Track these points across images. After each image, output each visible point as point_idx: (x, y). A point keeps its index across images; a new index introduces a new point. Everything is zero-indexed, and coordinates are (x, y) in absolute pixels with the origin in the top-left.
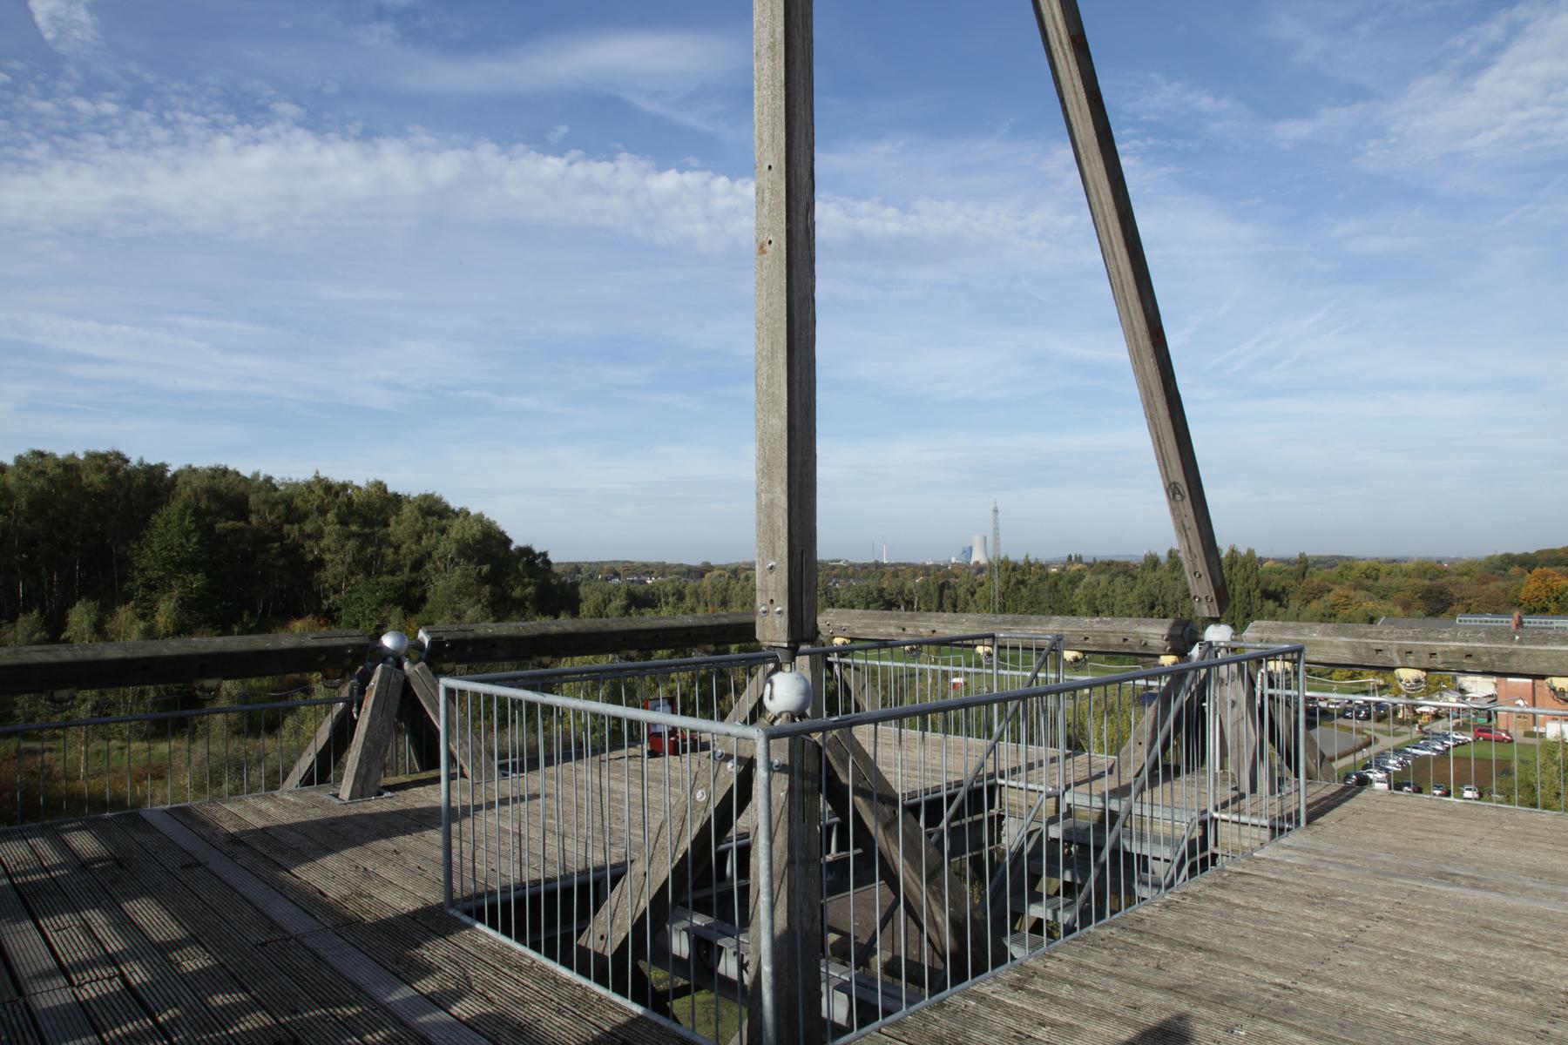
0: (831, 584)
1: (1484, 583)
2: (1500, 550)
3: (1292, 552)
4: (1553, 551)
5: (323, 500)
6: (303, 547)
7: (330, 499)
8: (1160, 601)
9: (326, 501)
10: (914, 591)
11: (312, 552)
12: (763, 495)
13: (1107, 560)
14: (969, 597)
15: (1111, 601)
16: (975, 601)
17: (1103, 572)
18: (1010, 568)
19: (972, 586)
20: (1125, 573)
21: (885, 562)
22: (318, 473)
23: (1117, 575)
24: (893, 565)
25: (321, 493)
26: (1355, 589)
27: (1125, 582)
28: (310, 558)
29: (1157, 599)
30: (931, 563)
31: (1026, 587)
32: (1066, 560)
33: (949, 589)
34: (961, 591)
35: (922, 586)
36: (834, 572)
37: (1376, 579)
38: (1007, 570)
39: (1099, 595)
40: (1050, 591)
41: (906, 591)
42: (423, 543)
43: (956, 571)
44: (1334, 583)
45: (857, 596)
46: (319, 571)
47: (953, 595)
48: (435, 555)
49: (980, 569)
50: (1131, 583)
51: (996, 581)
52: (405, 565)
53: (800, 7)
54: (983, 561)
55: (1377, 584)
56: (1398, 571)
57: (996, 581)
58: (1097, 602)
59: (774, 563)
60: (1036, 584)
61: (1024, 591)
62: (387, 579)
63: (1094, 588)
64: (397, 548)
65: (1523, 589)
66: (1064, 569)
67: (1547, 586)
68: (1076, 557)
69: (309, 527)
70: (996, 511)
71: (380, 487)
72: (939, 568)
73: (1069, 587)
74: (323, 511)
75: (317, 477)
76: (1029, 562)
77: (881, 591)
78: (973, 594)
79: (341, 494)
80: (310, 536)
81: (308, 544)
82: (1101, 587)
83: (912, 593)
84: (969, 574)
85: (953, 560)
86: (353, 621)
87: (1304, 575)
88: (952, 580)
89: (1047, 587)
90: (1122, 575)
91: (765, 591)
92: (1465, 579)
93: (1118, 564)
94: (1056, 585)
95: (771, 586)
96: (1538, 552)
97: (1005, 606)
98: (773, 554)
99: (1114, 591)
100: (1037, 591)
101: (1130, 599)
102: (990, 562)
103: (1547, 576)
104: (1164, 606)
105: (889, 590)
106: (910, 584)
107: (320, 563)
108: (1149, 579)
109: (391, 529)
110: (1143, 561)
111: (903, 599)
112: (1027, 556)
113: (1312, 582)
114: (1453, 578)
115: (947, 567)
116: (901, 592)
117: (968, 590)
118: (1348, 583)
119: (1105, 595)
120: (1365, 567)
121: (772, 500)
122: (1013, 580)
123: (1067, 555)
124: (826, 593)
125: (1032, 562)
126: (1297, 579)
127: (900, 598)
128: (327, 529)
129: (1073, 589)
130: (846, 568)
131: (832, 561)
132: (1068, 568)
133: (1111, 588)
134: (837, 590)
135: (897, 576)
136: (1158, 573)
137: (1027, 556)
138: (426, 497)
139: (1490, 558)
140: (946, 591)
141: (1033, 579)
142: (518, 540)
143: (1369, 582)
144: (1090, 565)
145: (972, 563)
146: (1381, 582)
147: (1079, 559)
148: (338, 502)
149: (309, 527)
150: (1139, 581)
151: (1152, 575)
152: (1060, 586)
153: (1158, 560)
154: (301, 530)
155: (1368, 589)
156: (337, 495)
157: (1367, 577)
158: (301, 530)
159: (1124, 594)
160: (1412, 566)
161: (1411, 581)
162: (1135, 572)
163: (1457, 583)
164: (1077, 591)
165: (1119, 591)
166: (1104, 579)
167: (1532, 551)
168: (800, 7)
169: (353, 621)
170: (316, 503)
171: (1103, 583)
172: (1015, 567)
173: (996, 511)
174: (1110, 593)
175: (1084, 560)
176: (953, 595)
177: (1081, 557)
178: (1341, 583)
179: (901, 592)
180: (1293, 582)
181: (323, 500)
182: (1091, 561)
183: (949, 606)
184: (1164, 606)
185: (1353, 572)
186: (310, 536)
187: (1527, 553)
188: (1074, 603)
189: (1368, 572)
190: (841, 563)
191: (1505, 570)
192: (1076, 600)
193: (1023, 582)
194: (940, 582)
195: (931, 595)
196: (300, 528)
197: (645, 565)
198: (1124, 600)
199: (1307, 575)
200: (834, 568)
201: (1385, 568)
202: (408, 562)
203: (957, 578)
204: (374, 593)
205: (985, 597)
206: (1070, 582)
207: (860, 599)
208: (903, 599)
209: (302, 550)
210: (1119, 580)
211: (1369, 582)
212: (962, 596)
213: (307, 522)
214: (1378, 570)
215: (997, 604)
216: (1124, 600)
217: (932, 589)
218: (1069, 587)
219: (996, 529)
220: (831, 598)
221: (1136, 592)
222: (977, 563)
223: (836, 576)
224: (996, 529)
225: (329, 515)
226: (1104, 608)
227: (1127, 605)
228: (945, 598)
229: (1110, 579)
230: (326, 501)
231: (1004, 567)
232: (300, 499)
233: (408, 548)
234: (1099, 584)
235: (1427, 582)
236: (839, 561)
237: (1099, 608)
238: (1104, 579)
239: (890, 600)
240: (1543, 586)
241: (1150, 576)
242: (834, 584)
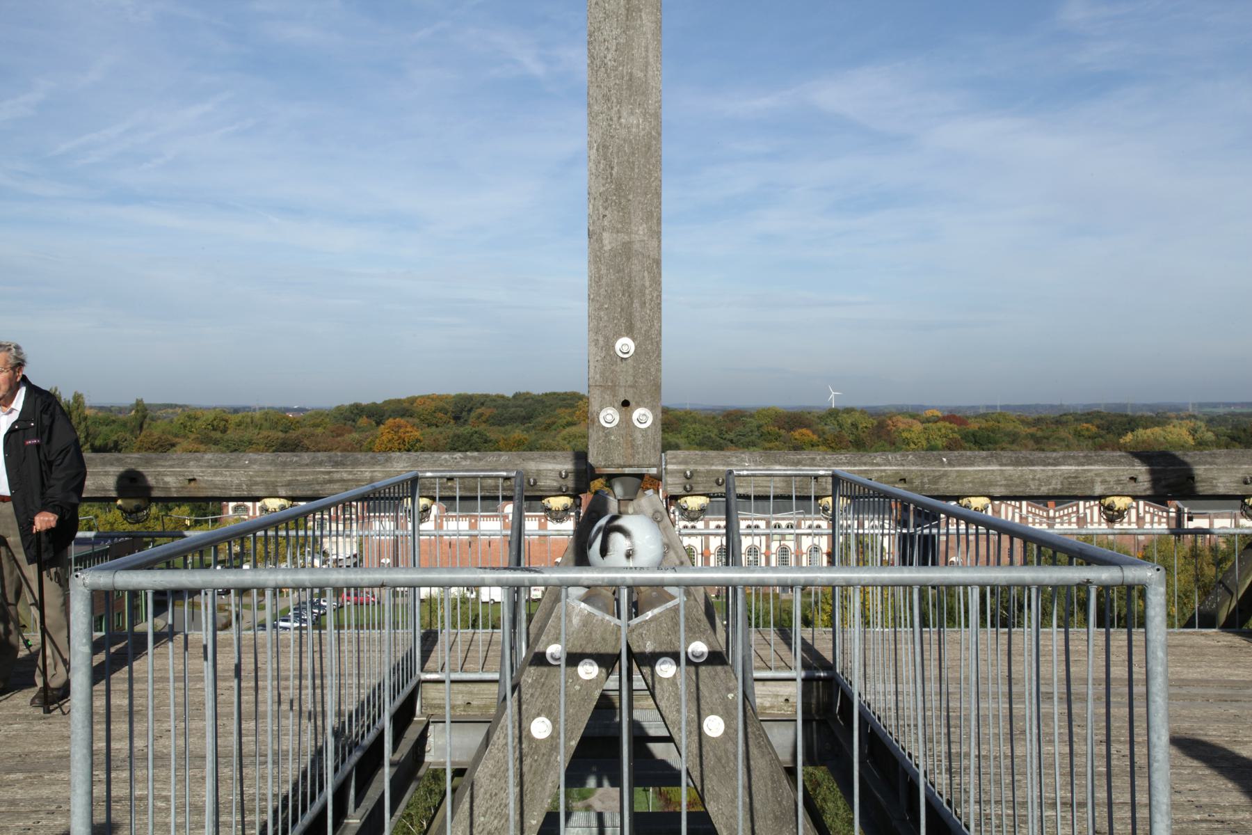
1: (338, 435)
2: (348, 401)
3: (128, 400)
4: (399, 401)
26: (202, 443)
37: (224, 431)
44: (176, 436)
55: (226, 437)
56: (249, 420)
65: (377, 441)
67: (400, 437)
87: (141, 427)
92: (320, 430)
96: (385, 402)
103: (399, 427)
113: (151, 435)
114: (308, 430)
118: (193, 436)
120: (211, 417)
126: (132, 432)
139: (338, 408)
143: (218, 435)
146: (231, 434)
155: (216, 442)
157: (214, 429)
160: (257, 415)
161: (265, 433)
163: (313, 435)
167: (379, 401)
178: (185, 437)
180: (128, 435)
185: (198, 423)
187: (375, 404)
189: (215, 423)
191: (354, 421)
199: (145, 426)
201: (235, 418)
211: (218, 435)
214: (227, 421)
235: (281, 435)
240: (396, 437)
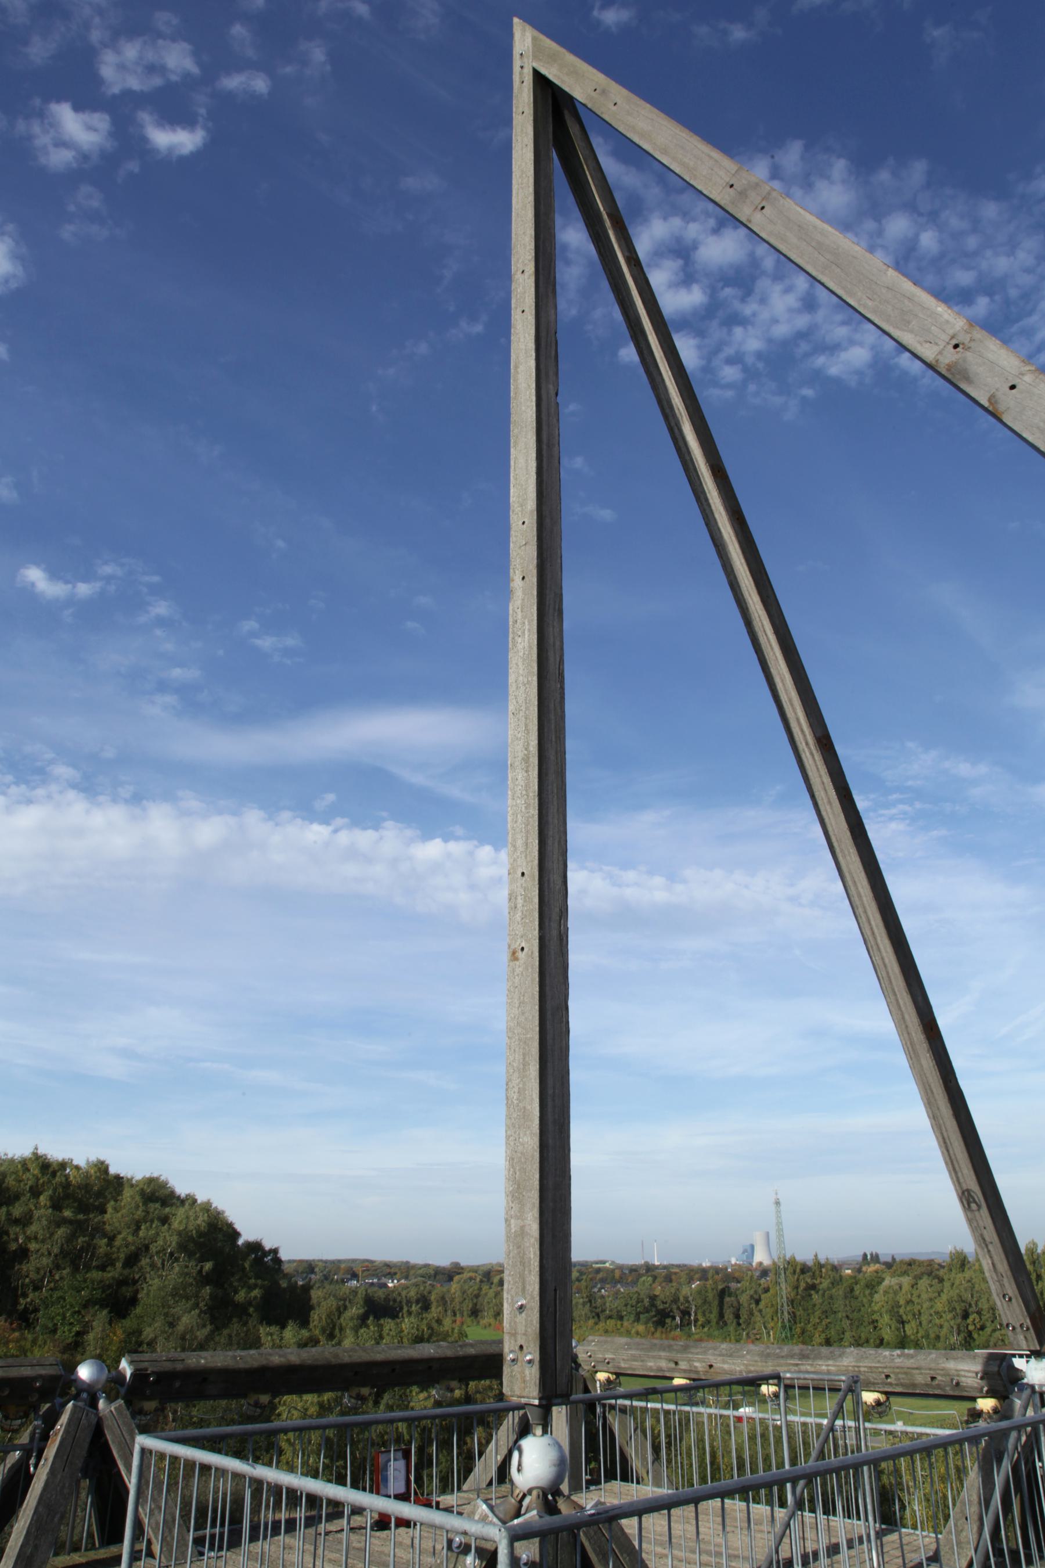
0: (596, 1290)
5: (38, 1179)
6: (7, 1233)
7: (46, 1179)
8: (974, 1309)
9: (41, 1181)
10: (690, 1299)
11: (17, 1240)
12: (513, 1221)
13: (907, 1258)
14: (753, 1306)
15: (917, 1308)
16: (760, 1311)
17: (905, 1273)
18: (798, 1270)
19: (756, 1292)
20: (930, 1274)
21: (657, 1263)
22: (36, 1149)
23: (918, 1278)
24: (665, 1267)
25: (37, 1172)
27: (931, 1286)
28: (13, 1246)
29: (970, 1305)
30: (708, 1264)
31: (817, 1292)
32: (860, 1259)
33: (730, 1295)
34: (744, 1299)
35: (699, 1292)
36: (600, 1276)
38: (794, 1272)
39: (902, 1302)
40: (846, 1297)
41: (682, 1299)
42: (141, 1234)
43: (737, 1275)
45: (626, 1305)
46: (20, 1263)
47: (735, 1304)
48: (153, 1248)
49: (765, 1272)
50: (938, 1287)
51: (783, 1286)
52: (118, 1258)
53: (553, 722)
54: (767, 1262)
57: (783, 1286)
58: (901, 1311)
59: (524, 1302)
60: (829, 1289)
61: (815, 1297)
62: (96, 1275)
63: (895, 1293)
64: (112, 1239)
66: (859, 1270)
68: (872, 1255)
69: (17, 1211)
70: (778, 1203)
71: (102, 1167)
72: (717, 1270)
73: (867, 1292)
74: (35, 1192)
75: (35, 1154)
76: (819, 1263)
77: (653, 1298)
78: (758, 1302)
79: (58, 1174)
80: (17, 1222)
81: (14, 1230)
82: (904, 1291)
83: (688, 1301)
84: (752, 1277)
85: (733, 1261)
86: (50, 1325)
88: (733, 1285)
89: (841, 1293)
90: (925, 1277)
91: (514, 1335)
93: (920, 1263)
94: (852, 1290)
95: (521, 1329)
97: (795, 1316)
98: (524, 1289)
99: (919, 1296)
100: (831, 1297)
101: (939, 1306)
102: (774, 1263)
104: (979, 1313)
105: (662, 1297)
106: (685, 1291)
107: (23, 1253)
108: (957, 1282)
109: (107, 1216)
110: (948, 1260)
111: (678, 1308)
112: (816, 1256)
115: (726, 1269)
116: (676, 1300)
117: (752, 1297)
119: (909, 1302)
121: (522, 1228)
122: (803, 1285)
123: (862, 1253)
124: (590, 1301)
125: (823, 1262)
127: (674, 1307)
128: (37, 1214)
129: (871, 1295)
130: (613, 1271)
131: (597, 1263)
132: (864, 1269)
133: (915, 1293)
134: (603, 1297)
135: (671, 1281)
136: (968, 1274)
137: (816, 1256)
138: (151, 1181)
140: (727, 1299)
141: (825, 1284)
142: (247, 1234)
144: (889, 1265)
145: (754, 1264)
147: (875, 1258)
148: (54, 1182)
149: (17, 1211)
150: (947, 1284)
151: (960, 1275)
152: (857, 1289)
153: (965, 1257)
154: (9, 1214)
156: (54, 1174)
158: (9, 1214)
159: (931, 1300)
162: (941, 1273)
164: (877, 1297)
165: (924, 1296)
166: (906, 1281)
168: (553, 722)
169: (50, 1325)
170: (30, 1183)
171: (906, 1287)
172: (804, 1269)
173: (778, 1203)
174: (915, 1299)
175: (882, 1259)
176: (735, 1304)
177: (877, 1256)
179: (676, 1300)
181: (38, 1179)
182: (889, 1260)
183: (731, 1316)
184: (979, 1313)
186: (17, 1222)
188: (874, 1312)
190: (607, 1265)
192: (876, 1308)
193: (813, 1287)
194: (720, 1287)
195: (710, 1304)
196: (8, 1211)
197: (387, 1265)
198: (932, 1307)
200: (598, 1270)
202: (122, 1256)
203: (739, 1282)
204: (79, 1291)
205: (772, 1305)
206: (867, 1286)
207: (629, 1308)
208: (678, 1308)
209: (5, 1238)
210: (924, 1282)
212: (746, 1305)
213: (17, 1205)
215: (786, 1313)
216: (932, 1307)
217: (710, 1296)
218: (867, 1292)
219: (779, 1224)
220: (596, 1308)
221: (944, 1297)
222: (761, 1263)
223: (603, 1281)
224: (779, 1224)
225: (42, 1198)
226: (910, 1317)
227: (937, 1313)
228: (725, 1307)
229: (913, 1282)
230: (41, 1181)
231: (790, 1270)
232: (13, 1177)
233: (124, 1239)
234: (901, 1288)
236: (604, 1262)
237: (904, 1317)
238: (906, 1281)
239: (664, 1310)
241: (959, 1278)
242: (600, 1291)
